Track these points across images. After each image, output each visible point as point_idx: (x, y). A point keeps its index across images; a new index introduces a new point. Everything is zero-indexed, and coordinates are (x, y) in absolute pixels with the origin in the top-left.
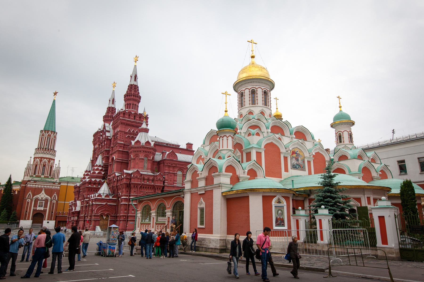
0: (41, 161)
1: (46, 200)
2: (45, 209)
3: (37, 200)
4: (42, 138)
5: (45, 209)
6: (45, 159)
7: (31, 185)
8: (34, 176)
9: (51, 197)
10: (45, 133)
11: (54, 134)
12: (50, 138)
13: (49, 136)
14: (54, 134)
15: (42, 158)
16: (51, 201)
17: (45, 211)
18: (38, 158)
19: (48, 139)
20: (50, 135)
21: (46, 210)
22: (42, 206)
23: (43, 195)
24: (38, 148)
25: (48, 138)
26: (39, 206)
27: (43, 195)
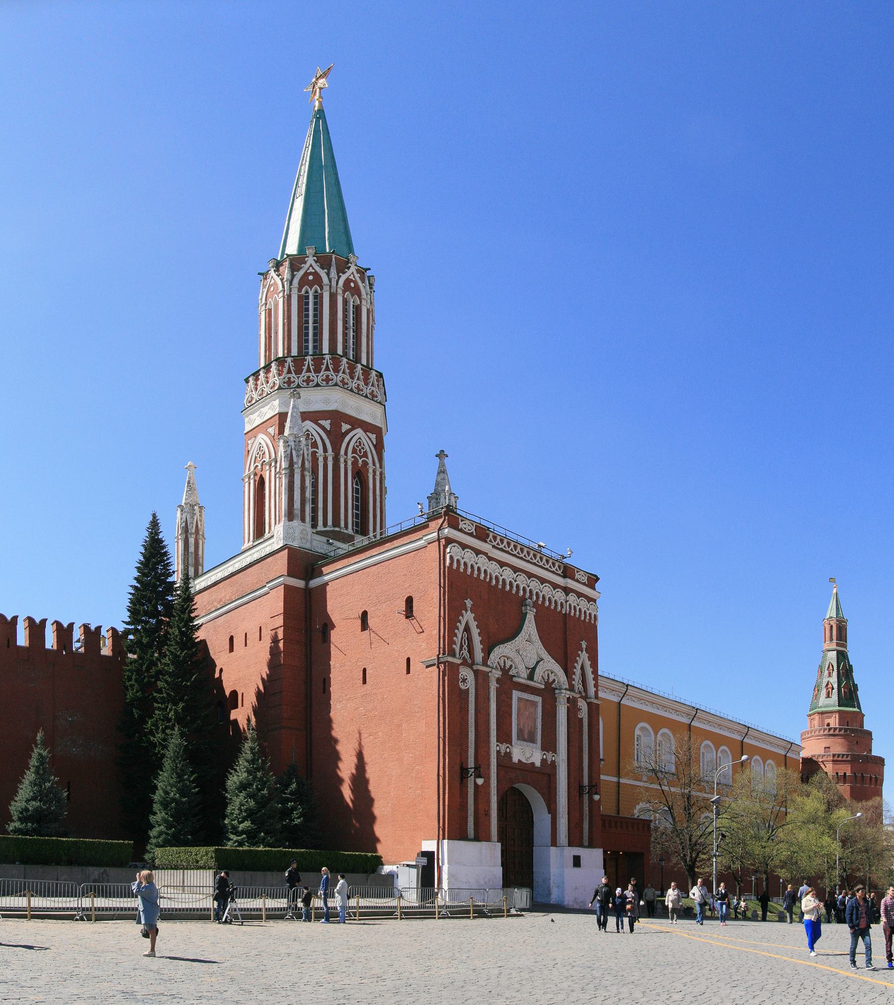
1: (549, 692)
2: (549, 757)
3: (507, 682)
5: (549, 757)
7: (469, 557)
9: (568, 673)
13: (351, 288)
16: (572, 704)
17: (548, 772)
20: (356, 291)
21: (553, 765)
22: (531, 739)
23: (526, 651)
25: (345, 302)
26: (521, 737)
27: (526, 651)
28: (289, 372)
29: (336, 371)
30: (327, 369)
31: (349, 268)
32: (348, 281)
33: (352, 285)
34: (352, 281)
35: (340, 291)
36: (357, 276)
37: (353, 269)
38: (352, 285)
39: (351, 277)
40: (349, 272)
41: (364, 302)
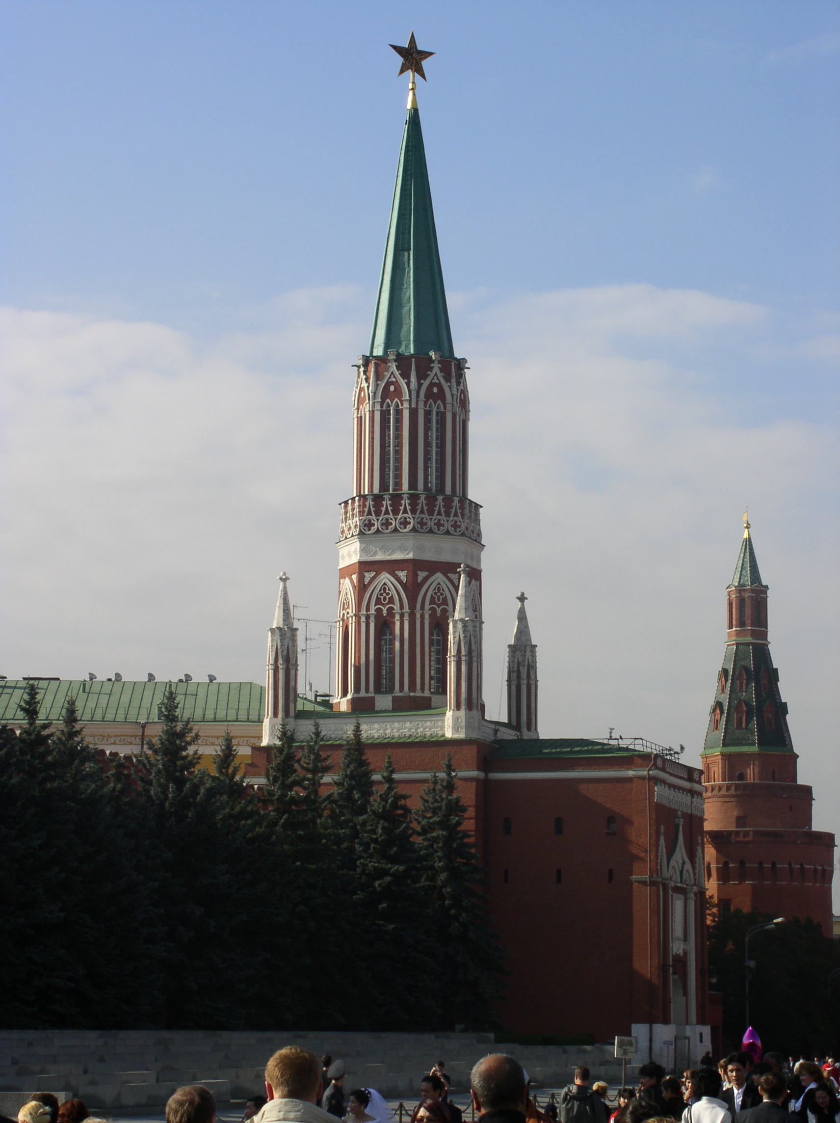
0: (412, 589)
4: (385, 415)
6: (439, 577)
8: (384, 702)
10: (406, 375)
11: (458, 384)
12: (442, 417)
13: (435, 395)
14: (458, 384)
15: (415, 565)
18: (391, 566)
19: (428, 421)
20: (441, 395)
24: (378, 499)
25: (428, 414)
28: (369, 513)
29: (413, 511)
30: (405, 511)
31: (431, 369)
32: (432, 385)
33: (435, 390)
34: (435, 385)
35: (421, 405)
36: (440, 375)
37: (436, 367)
38: (435, 390)
39: (435, 381)
40: (432, 375)
41: (449, 407)
